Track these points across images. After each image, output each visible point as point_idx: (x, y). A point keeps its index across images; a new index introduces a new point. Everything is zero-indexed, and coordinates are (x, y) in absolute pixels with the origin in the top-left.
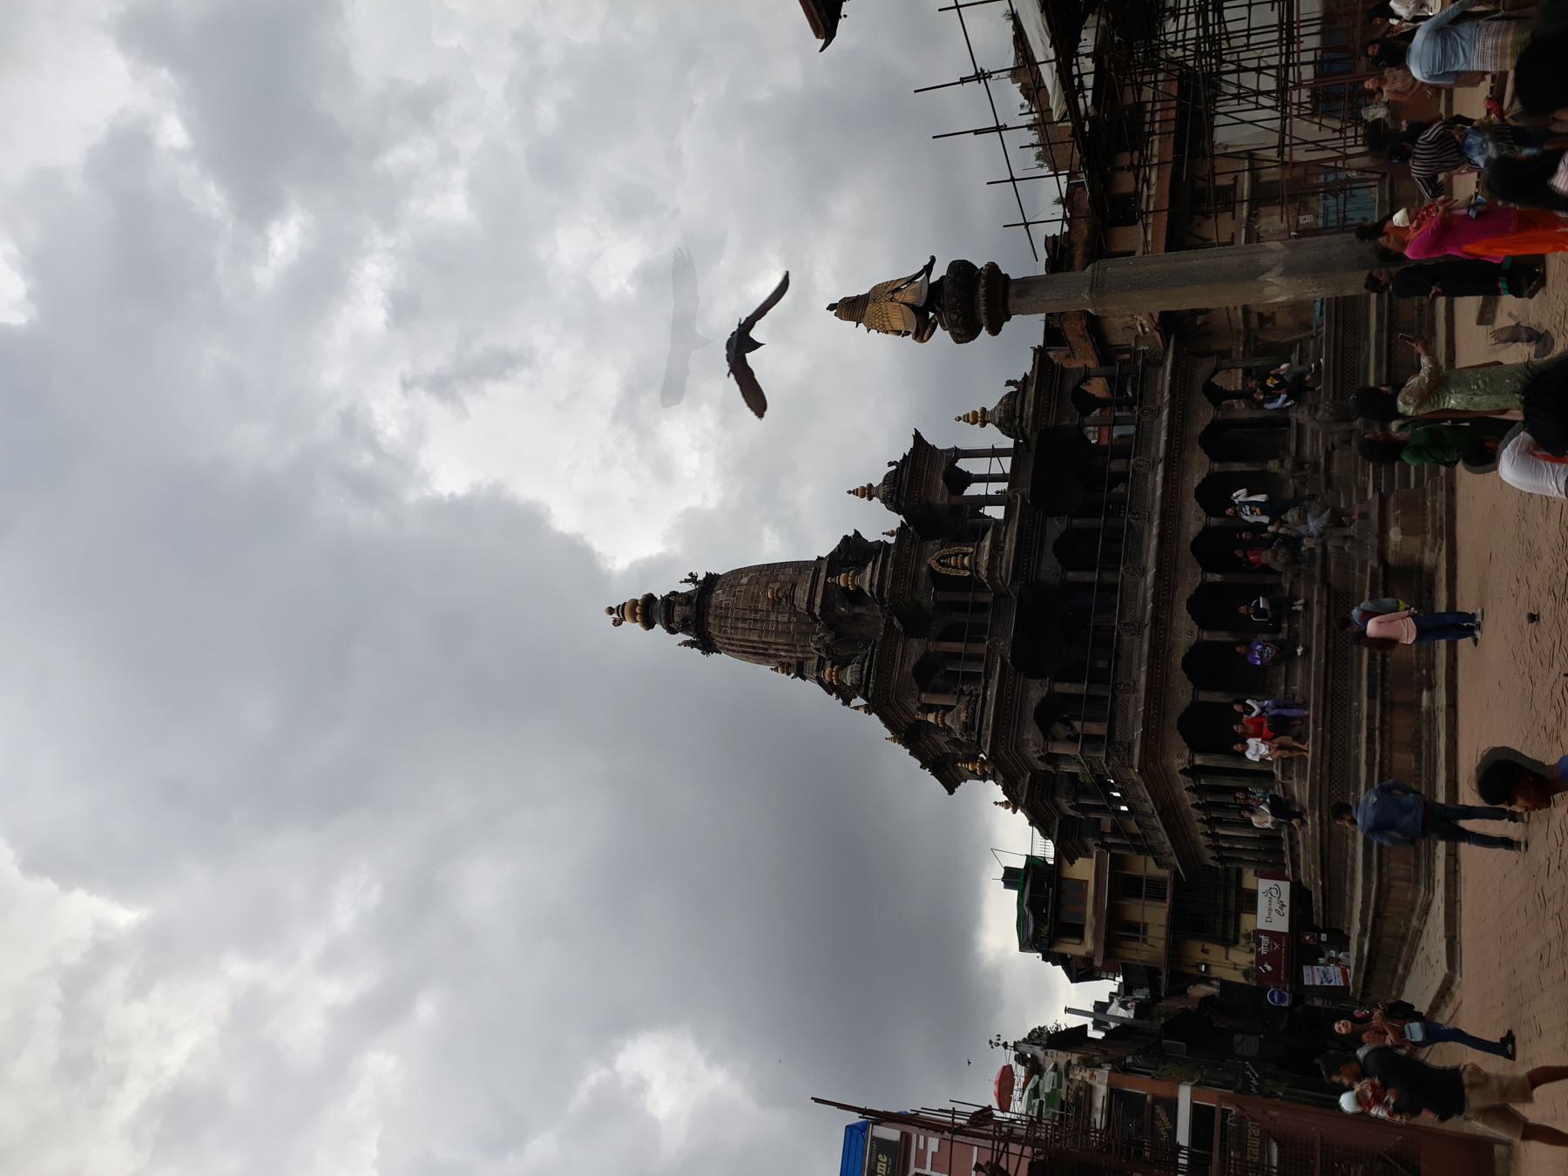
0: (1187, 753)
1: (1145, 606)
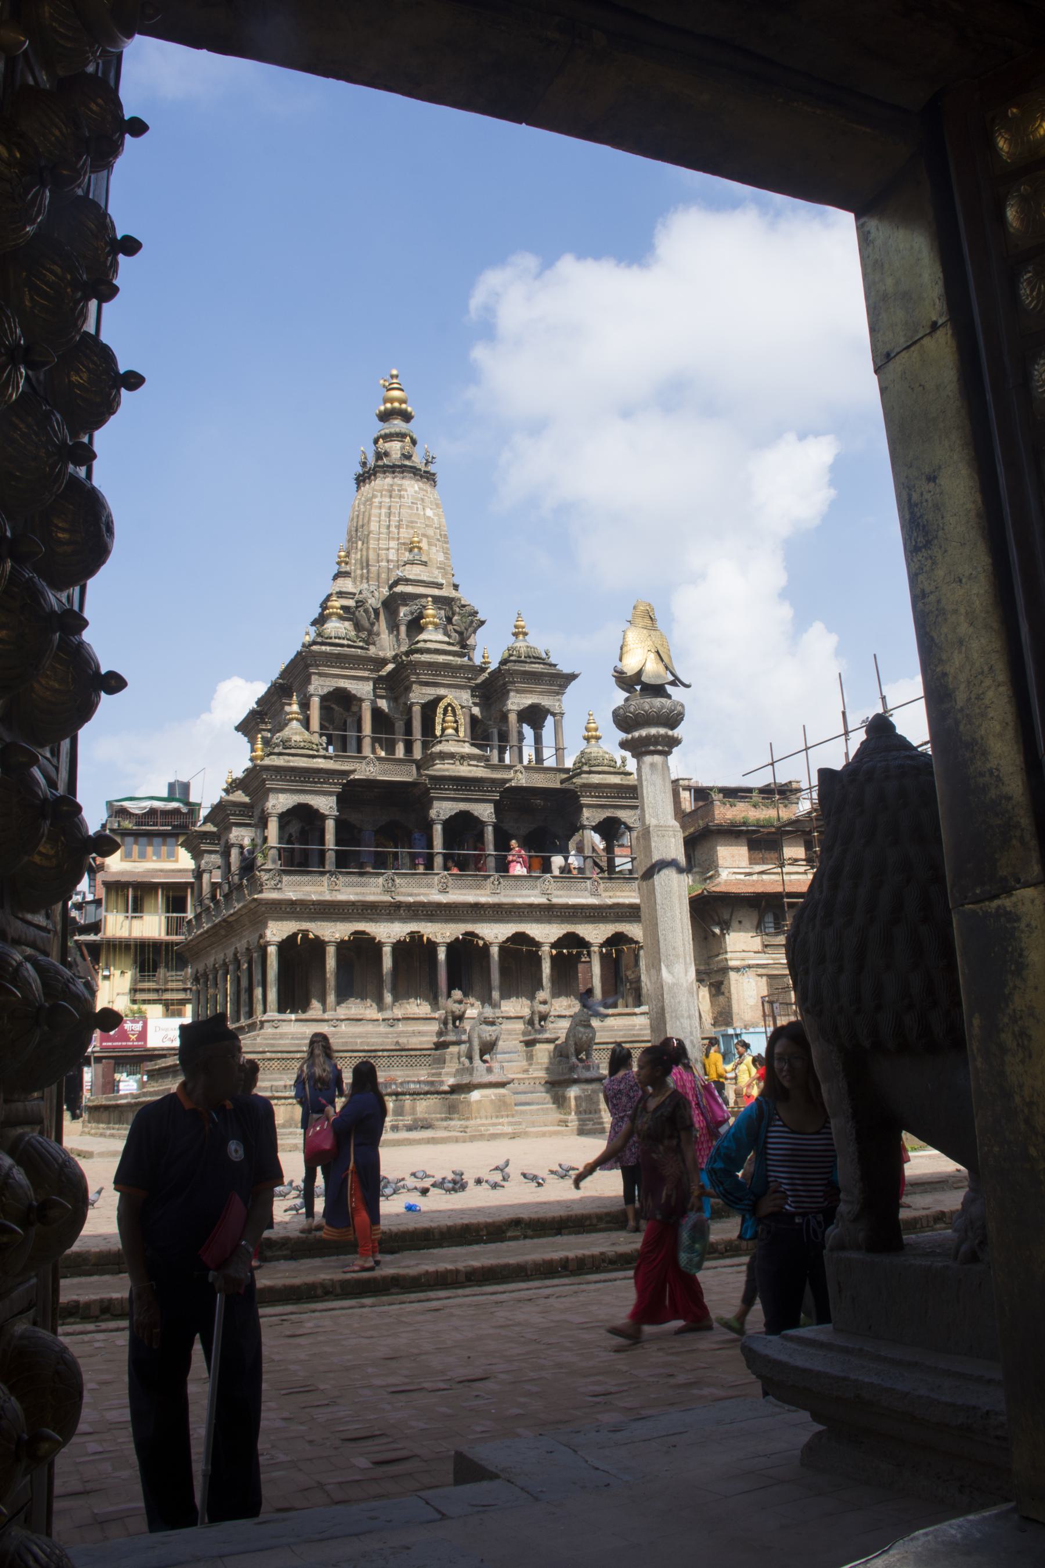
0: (278, 939)
1: (411, 895)
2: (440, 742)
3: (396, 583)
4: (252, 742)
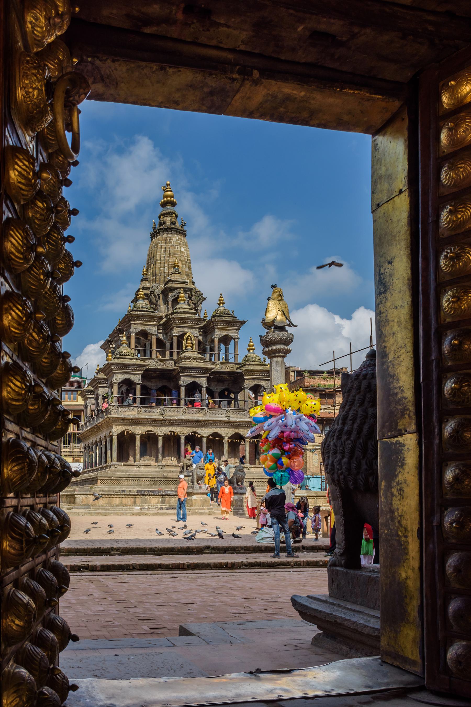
1: (170, 416)
2: (185, 352)
3: (168, 282)
4: (107, 353)
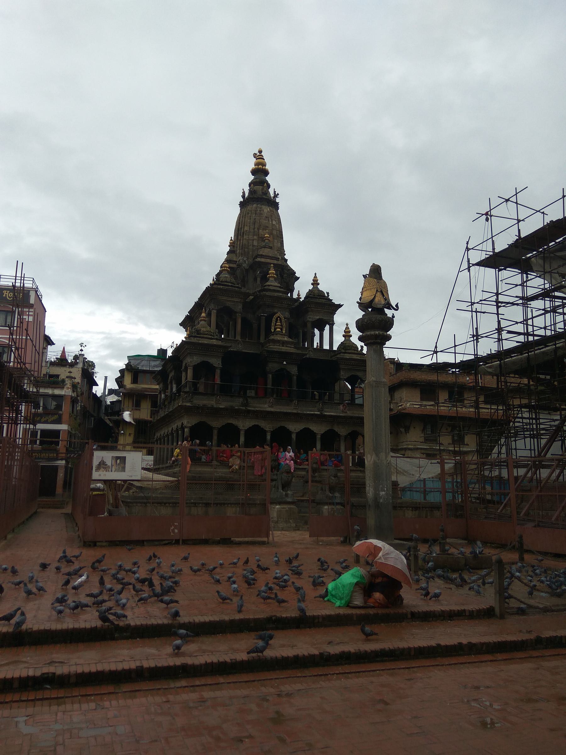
2: (273, 335)
